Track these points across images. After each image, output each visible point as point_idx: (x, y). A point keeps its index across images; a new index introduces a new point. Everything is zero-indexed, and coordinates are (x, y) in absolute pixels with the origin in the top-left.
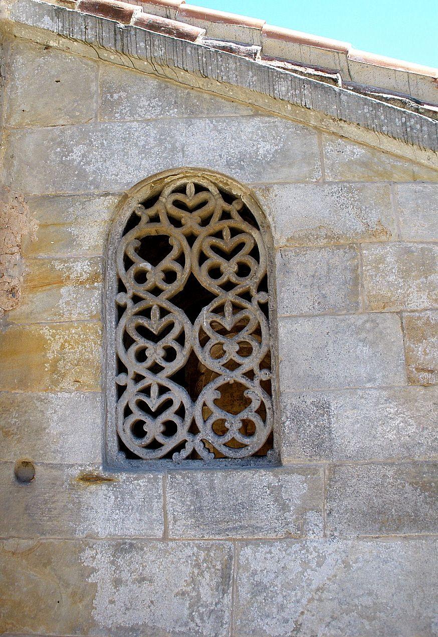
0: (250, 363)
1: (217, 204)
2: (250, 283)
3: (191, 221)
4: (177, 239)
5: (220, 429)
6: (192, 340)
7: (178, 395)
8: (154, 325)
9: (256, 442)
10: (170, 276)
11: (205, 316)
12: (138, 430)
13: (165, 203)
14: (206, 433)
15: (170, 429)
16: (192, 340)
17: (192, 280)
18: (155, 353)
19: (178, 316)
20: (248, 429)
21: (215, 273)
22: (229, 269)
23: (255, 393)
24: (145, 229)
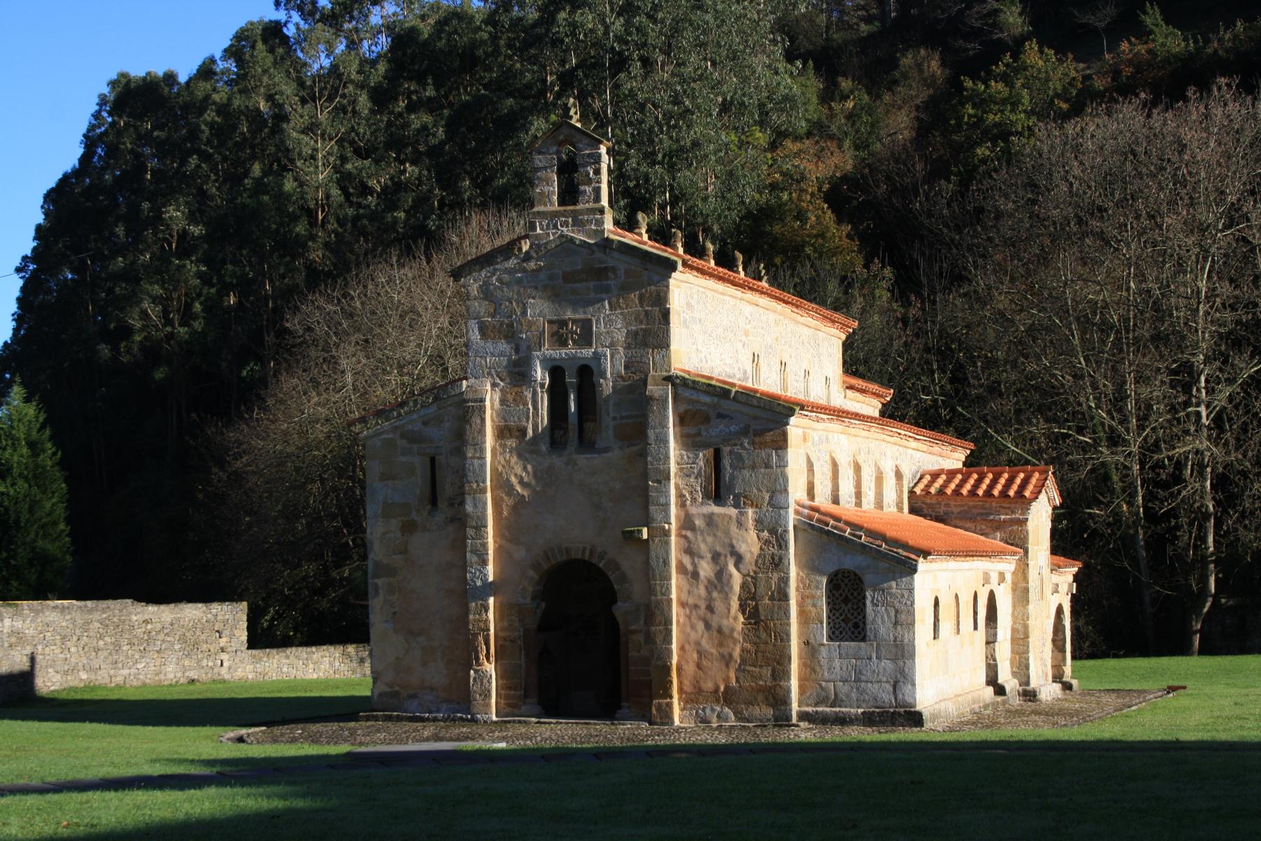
0: (860, 617)
1: (853, 577)
2: (860, 597)
3: (846, 581)
4: (843, 586)
5: (853, 633)
6: (846, 611)
7: (843, 625)
8: (837, 607)
9: (861, 636)
10: (841, 595)
11: (850, 605)
12: (833, 633)
13: (840, 576)
14: (849, 633)
15: (841, 633)
16: (846, 611)
17: (847, 596)
18: (837, 614)
19: (843, 605)
20: (860, 633)
21: (852, 594)
22: (855, 594)
23: (861, 624)
24: (835, 582)
